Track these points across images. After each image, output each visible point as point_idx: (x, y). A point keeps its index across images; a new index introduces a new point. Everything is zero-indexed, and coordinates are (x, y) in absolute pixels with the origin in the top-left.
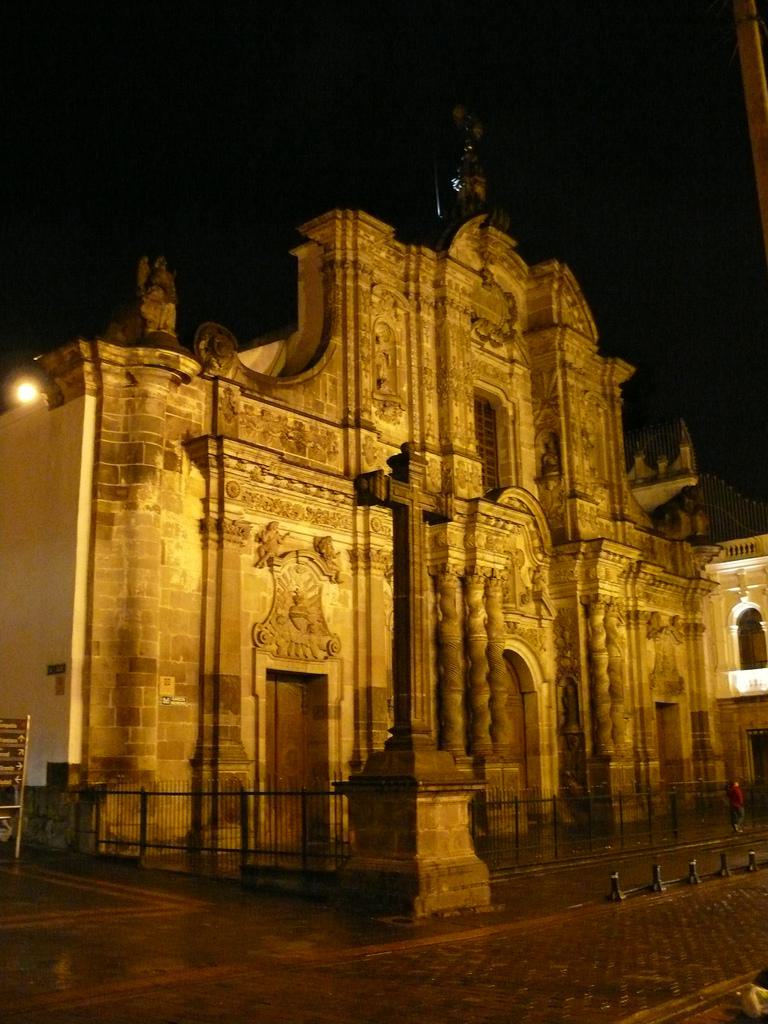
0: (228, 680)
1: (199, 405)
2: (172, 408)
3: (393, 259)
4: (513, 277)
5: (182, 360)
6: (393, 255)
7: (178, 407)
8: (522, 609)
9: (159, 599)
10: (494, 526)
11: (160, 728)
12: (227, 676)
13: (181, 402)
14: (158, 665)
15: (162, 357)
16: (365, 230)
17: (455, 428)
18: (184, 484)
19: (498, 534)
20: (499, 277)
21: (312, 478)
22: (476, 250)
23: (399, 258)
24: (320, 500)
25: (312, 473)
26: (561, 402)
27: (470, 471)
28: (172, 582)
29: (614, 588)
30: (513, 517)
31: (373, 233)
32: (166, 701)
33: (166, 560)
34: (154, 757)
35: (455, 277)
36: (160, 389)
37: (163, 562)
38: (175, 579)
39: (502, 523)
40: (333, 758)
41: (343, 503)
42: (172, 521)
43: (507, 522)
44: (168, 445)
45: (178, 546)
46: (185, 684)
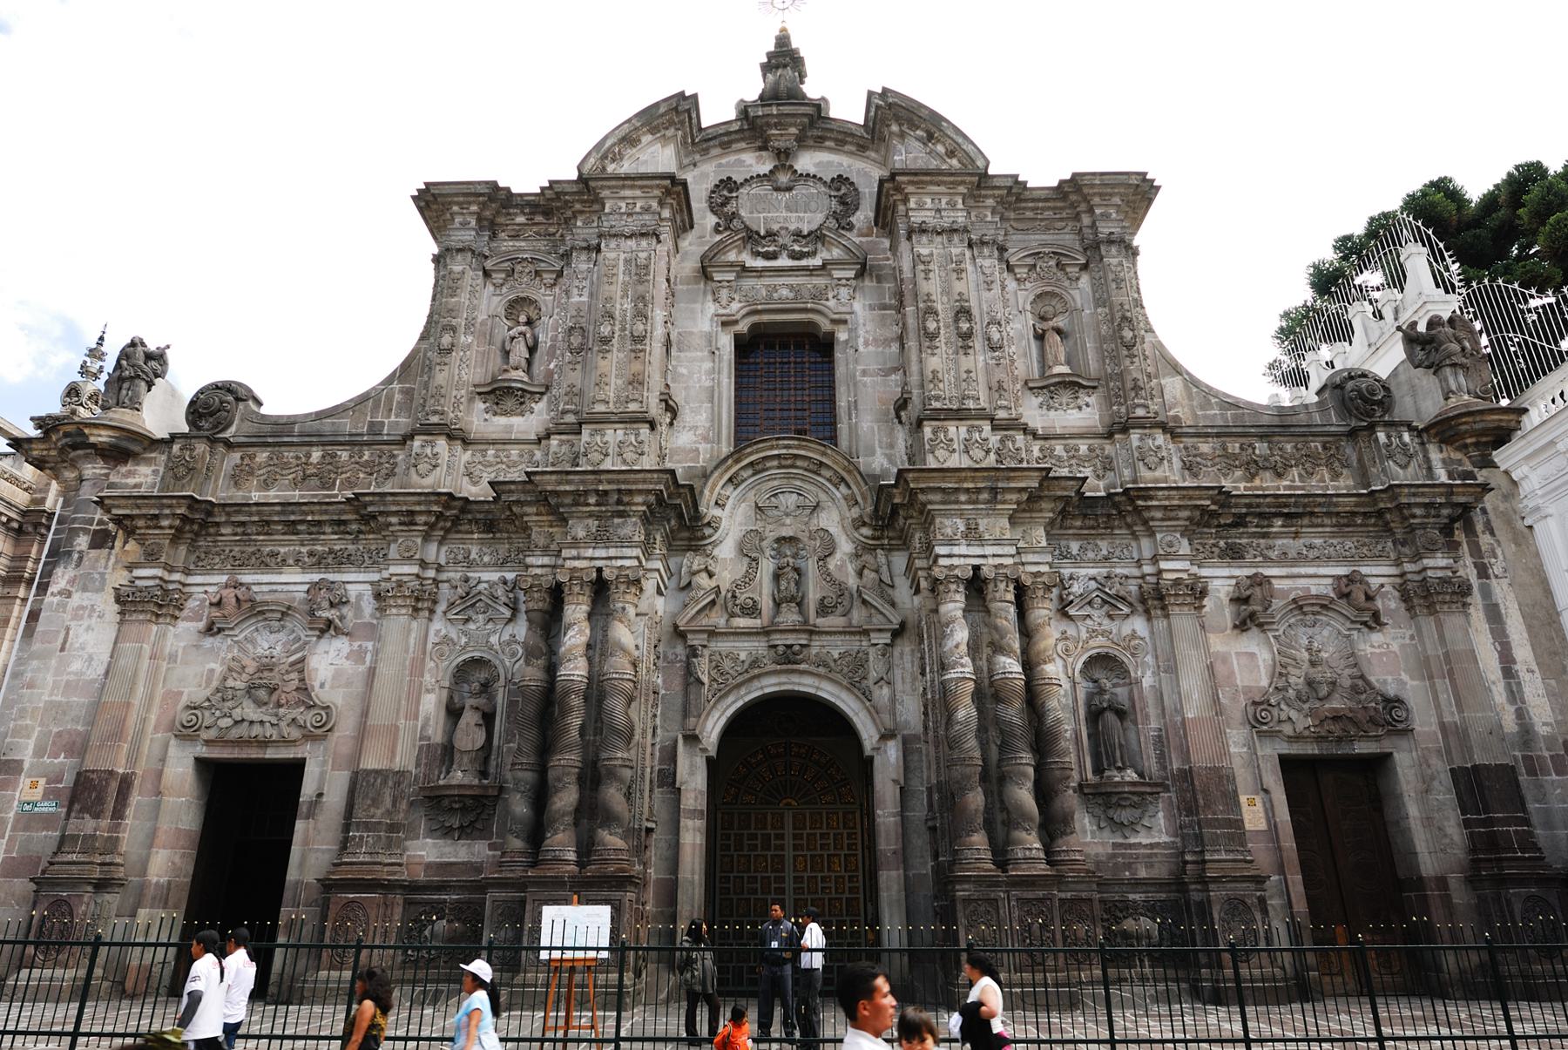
1: (155, 472)
3: (539, 218)
4: (852, 153)
8: (820, 621)
9: (47, 692)
10: (598, 504)
12: (93, 771)
14: (26, 766)
19: (622, 514)
20: (818, 165)
24: (322, 537)
26: (907, 287)
28: (69, 670)
29: (989, 550)
31: (470, 203)
32: (27, 807)
33: (67, 645)
35: (624, 198)
37: (62, 649)
40: (292, 875)
41: (360, 532)
43: (619, 491)
45: (89, 628)
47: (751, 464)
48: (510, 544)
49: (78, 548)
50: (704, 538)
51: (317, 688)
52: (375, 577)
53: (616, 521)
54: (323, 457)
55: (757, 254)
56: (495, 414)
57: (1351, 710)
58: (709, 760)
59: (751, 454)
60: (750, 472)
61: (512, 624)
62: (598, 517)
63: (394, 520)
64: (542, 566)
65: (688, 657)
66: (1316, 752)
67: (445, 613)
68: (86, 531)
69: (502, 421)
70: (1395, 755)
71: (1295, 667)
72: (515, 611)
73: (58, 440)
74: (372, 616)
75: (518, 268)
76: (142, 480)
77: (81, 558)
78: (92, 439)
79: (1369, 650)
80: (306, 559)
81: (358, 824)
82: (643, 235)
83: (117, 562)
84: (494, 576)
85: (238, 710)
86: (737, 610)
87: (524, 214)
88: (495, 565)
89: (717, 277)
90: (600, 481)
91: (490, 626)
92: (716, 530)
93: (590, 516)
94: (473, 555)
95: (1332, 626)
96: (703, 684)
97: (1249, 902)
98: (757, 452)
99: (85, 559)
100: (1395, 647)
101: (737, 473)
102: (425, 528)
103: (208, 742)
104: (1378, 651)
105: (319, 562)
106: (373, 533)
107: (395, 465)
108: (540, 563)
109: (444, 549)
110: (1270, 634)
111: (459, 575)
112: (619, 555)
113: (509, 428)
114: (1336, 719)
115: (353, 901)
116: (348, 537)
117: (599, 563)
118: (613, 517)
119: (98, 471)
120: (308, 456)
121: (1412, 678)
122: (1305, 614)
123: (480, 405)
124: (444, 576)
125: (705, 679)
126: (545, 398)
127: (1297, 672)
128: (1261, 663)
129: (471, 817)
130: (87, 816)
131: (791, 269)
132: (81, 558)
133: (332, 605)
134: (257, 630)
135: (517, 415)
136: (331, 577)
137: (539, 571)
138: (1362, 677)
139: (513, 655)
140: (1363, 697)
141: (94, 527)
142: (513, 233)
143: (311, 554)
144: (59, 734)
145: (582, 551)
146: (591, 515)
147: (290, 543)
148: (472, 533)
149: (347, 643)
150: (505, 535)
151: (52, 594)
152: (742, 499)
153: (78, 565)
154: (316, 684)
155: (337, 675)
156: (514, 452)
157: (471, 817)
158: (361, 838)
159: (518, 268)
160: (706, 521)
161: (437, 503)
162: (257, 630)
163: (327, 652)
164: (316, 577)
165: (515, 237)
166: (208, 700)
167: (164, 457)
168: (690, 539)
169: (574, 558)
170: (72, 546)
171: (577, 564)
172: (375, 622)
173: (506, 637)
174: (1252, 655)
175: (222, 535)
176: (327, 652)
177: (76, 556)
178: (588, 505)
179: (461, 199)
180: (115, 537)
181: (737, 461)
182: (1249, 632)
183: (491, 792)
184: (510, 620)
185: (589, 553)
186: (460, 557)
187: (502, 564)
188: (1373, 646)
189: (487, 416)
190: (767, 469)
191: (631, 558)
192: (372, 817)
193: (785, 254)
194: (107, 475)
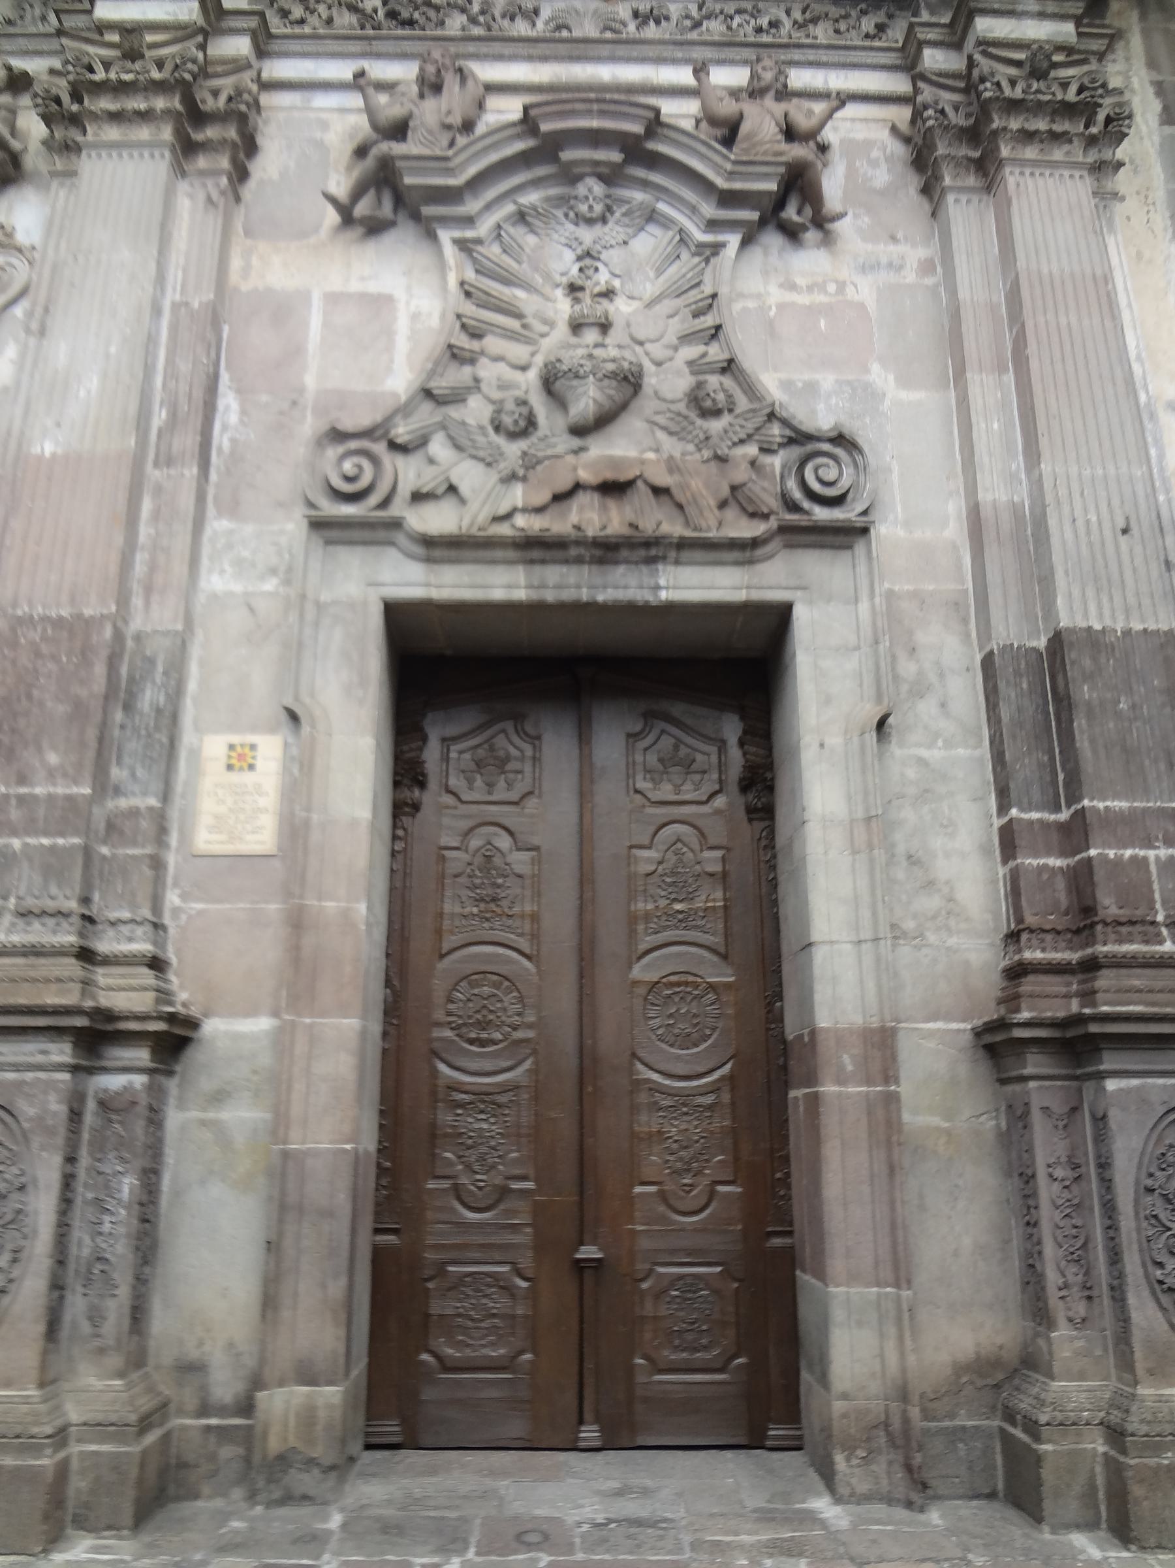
57: (672, 466)
66: (521, 595)
70: (800, 614)
71: (510, 335)
79: (775, 295)
95: (666, 223)
97: (27, 1109)
100: (864, 291)
104: (803, 299)
110: (445, 236)
114: (613, 489)
121: (904, 381)
122: (570, 176)
127: (518, 352)
128: (402, 325)
138: (729, 367)
140: (716, 426)
174: (381, 303)
182: (389, 239)
188: (792, 287)
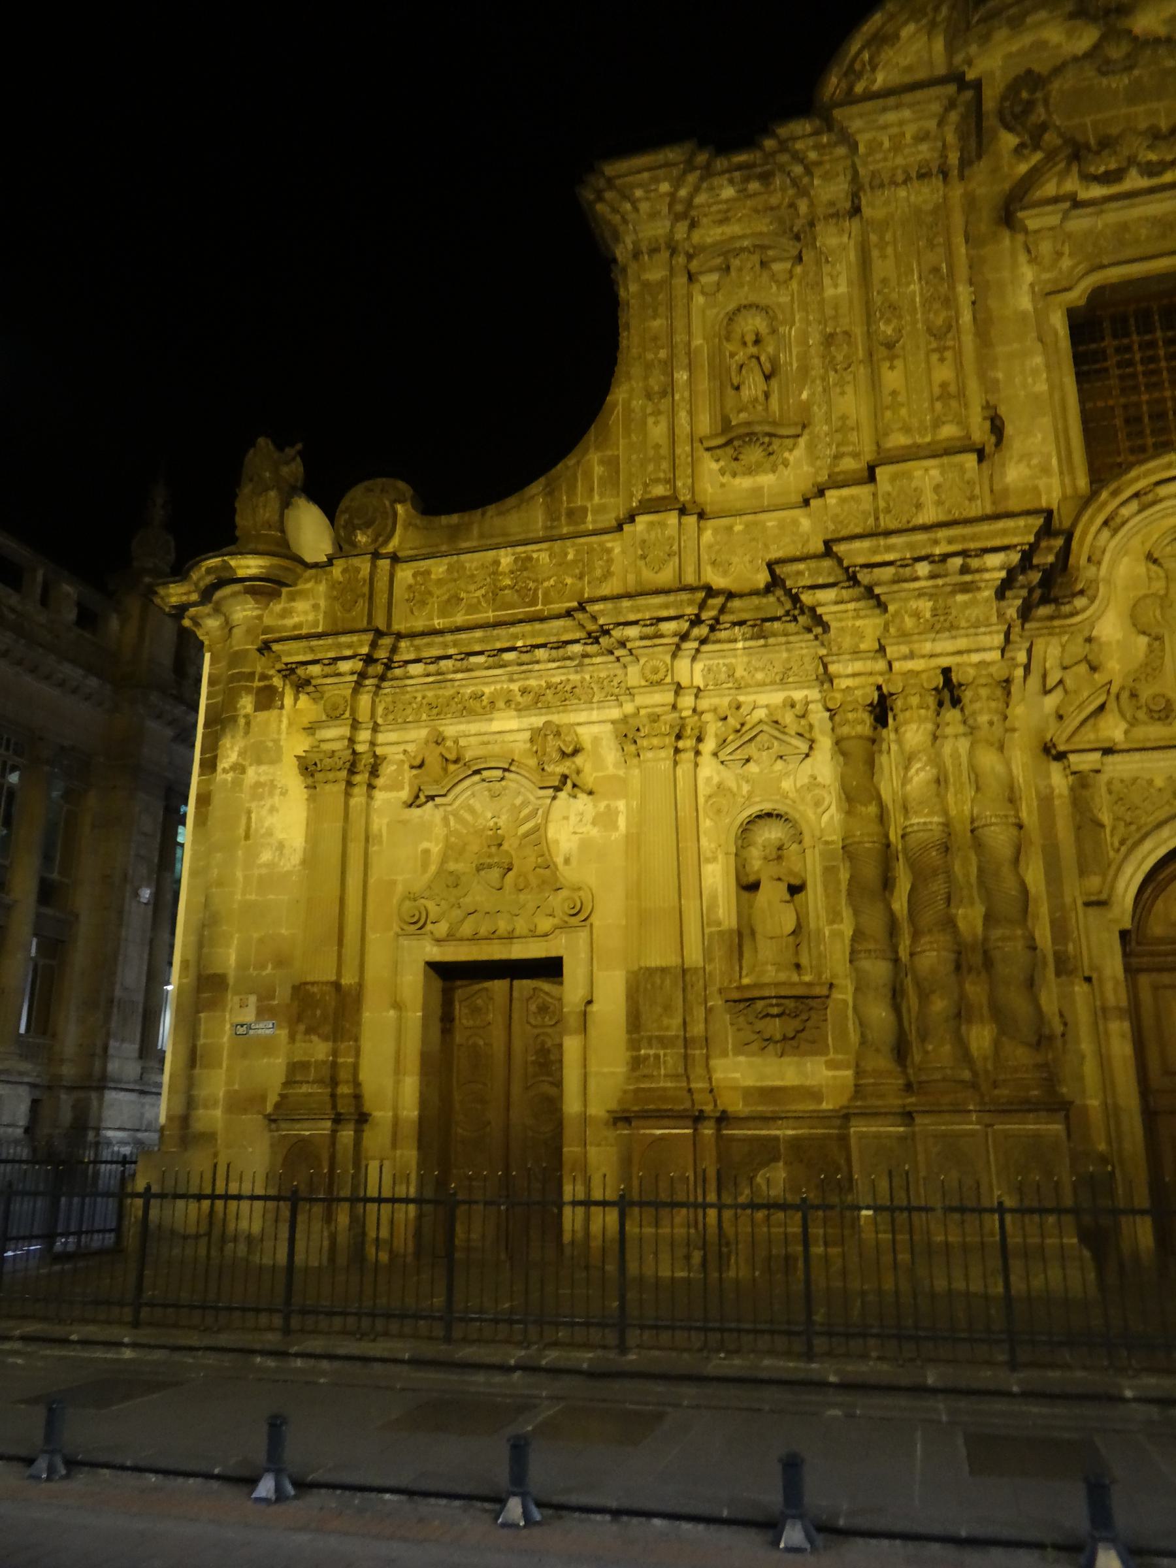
0: (315, 989)
1: (316, 607)
2: (268, 627)
3: (754, 186)
5: (233, 563)
6: (747, 180)
7: (280, 622)
10: (933, 576)
11: (228, 1069)
12: (313, 984)
13: (286, 613)
14: (231, 981)
15: (209, 571)
16: (640, 185)
17: (888, 414)
18: (285, 721)
19: (965, 588)
21: (481, 640)
22: (1072, 16)
23: (765, 178)
24: (537, 667)
25: (478, 634)
27: (939, 479)
30: (974, 538)
31: (656, 180)
32: (241, 1030)
34: (218, 1113)
35: (885, 127)
36: (245, 610)
37: (247, 837)
38: (266, 856)
39: (958, 561)
40: (572, 1106)
41: (585, 655)
42: (262, 779)
43: (964, 553)
44: (264, 677)
45: (273, 810)
46: (276, 1002)
47: (1137, 495)
48: (788, 650)
49: (243, 712)
50: (1072, 614)
51: (561, 866)
52: (615, 713)
53: (960, 598)
54: (516, 560)
55: (1088, 178)
56: (734, 475)
58: (1124, 935)
59: (1137, 479)
60: (1134, 506)
61: (809, 760)
62: (931, 596)
63: (632, 632)
64: (854, 675)
65: (1072, 789)
67: (715, 754)
68: (249, 690)
69: (745, 483)
72: (812, 743)
73: (200, 579)
74: (616, 765)
75: (735, 263)
76: (302, 618)
77: (248, 724)
78: (241, 573)
80: (519, 699)
81: (650, 1039)
82: (922, 176)
83: (290, 724)
84: (776, 698)
85: (468, 899)
86: (1141, 715)
87: (731, 182)
88: (773, 683)
89: (1032, 224)
90: (936, 542)
91: (779, 765)
92: (1092, 600)
93: (920, 596)
94: (740, 672)
96: (1102, 826)
98: (1146, 474)
99: (253, 723)
101: (1114, 514)
102: (676, 639)
103: (438, 941)
105: (537, 700)
106: (602, 654)
107: (610, 561)
108: (850, 670)
109: (699, 666)
111: (725, 701)
112: (973, 647)
113: (757, 491)
115: (662, 1138)
116: (568, 663)
117: (945, 662)
118: (953, 593)
119: (249, 613)
120: (497, 563)
123: (710, 465)
124: (704, 704)
125: (1106, 818)
126: (802, 442)
129: (796, 1024)
130: (315, 1038)
131: (1151, 190)
132: (248, 724)
133: (564, 755)
134: (473, 795)
135: (765, 472)
136: (555, 718)
137: (849, 682)
139: (817, 804)
141: (257, 684)
142: (719, 217)
143: (524, 691)
144: (261, 941)
145: (916, 646)
146: (921, 594)
147: (495, 680)
148: (735, 641)
149: (590, 806)
150: (783, 639)
151: (225, 771)
152: (1123, 551)
153: (247, 733)
154: (559, 860)
155: (586, 845)
156: (771, 521)
157: (796, 1024)
158: (657, 1057)
159: (735, 263)
160: (1080, 586)
161: (691, 602)
162: (473, 795)
163: (566, 818)
164: (538, 721)
165: (721, 222)
166: (429, 887)
167: (322, 588)
168: (1051, 618)
169: (905, 658)
170: (235, 709)
171: (910, 665)
172: (621, 773)
173: (803, 780)
175: (411, 677)
176: (566, 818)
177: (242, 721)
178: (917, 579)
179: (646, 175)
180: (283, 694)
181: (1115, 494)
183: (817, 991)
184: (807, 755)
185: (928, 647)
186: (723, 676)
187: (783, 682)
189: (724, 480)
190: (1161, 500)
191: (991, 649)
192: (668, 1028)
193: (1133, 172)
194: (260, 617)
